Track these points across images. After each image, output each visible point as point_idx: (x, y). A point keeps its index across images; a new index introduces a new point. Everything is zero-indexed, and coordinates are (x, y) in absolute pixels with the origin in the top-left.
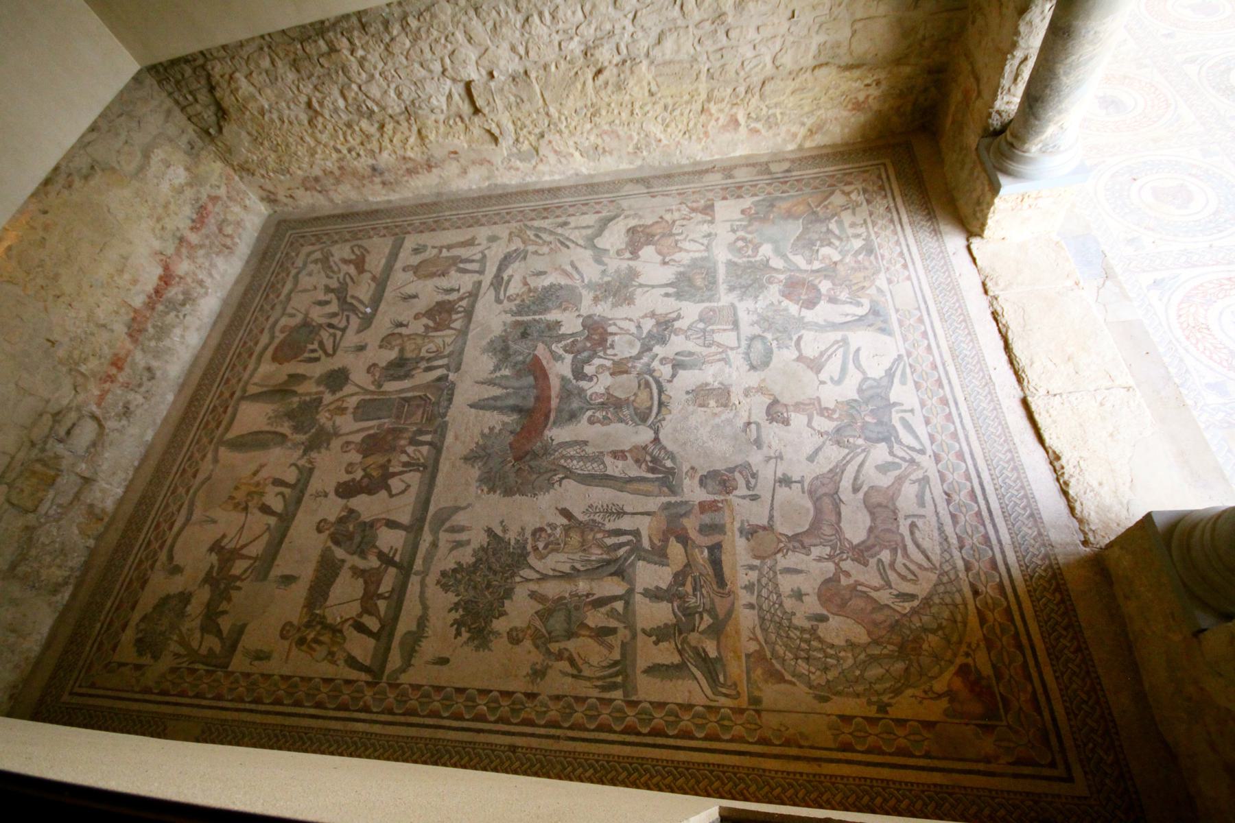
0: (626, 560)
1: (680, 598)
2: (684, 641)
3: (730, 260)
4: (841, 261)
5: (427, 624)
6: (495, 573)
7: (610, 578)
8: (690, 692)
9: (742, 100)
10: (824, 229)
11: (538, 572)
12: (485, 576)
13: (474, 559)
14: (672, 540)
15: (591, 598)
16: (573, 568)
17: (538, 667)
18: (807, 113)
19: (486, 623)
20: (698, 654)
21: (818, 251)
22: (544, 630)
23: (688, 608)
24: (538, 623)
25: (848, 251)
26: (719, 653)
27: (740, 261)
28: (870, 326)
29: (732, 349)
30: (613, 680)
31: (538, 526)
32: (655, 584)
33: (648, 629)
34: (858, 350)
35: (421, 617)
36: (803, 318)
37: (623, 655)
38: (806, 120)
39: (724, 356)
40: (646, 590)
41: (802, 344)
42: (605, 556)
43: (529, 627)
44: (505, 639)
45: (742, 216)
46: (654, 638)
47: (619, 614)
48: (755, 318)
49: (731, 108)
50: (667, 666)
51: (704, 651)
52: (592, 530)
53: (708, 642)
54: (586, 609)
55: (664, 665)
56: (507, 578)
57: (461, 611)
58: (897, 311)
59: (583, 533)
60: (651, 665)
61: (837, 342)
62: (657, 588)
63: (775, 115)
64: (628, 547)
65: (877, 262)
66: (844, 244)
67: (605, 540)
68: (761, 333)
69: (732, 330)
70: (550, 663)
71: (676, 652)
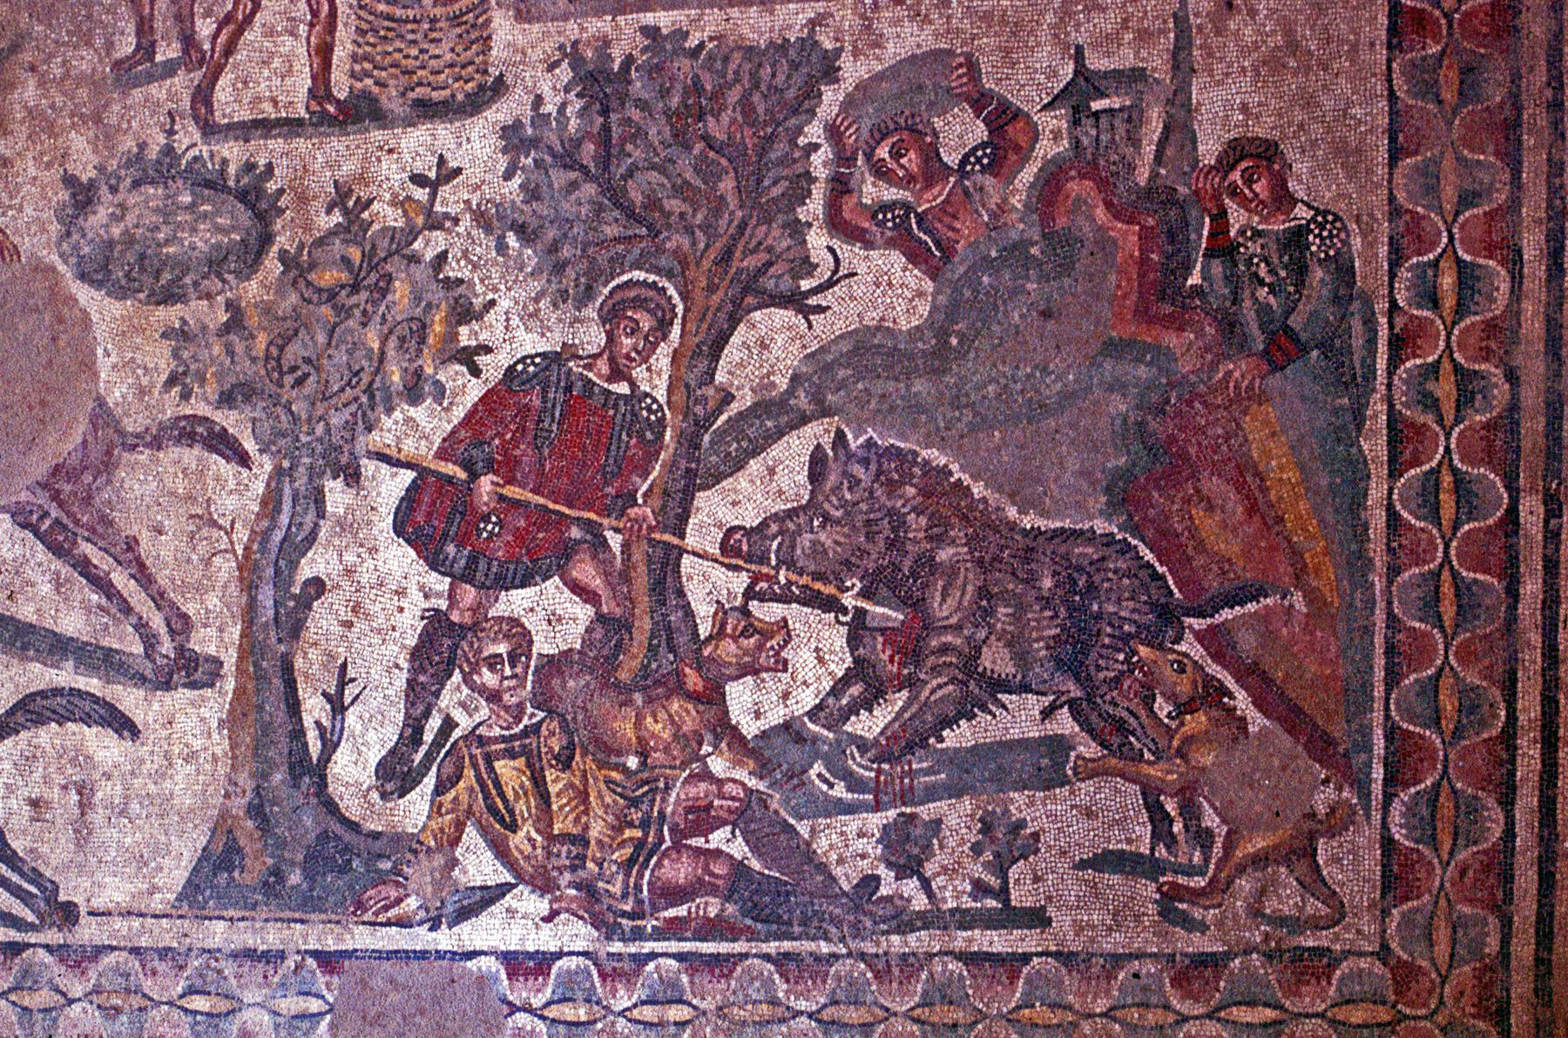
4: (725, 730)
10: (996, 660)
21: (830, 605)
25: (796, 776)
27: (814, 132)
28: (256, 810)
29: (203, 96)
34: (124, 726)
39: (167, 51)
41: (191, 455)
45: (1209, 149)
48: (387, 215)
58: (329, 961)
61: (181, 625)
65: (673, 929)
66: (859, 765)
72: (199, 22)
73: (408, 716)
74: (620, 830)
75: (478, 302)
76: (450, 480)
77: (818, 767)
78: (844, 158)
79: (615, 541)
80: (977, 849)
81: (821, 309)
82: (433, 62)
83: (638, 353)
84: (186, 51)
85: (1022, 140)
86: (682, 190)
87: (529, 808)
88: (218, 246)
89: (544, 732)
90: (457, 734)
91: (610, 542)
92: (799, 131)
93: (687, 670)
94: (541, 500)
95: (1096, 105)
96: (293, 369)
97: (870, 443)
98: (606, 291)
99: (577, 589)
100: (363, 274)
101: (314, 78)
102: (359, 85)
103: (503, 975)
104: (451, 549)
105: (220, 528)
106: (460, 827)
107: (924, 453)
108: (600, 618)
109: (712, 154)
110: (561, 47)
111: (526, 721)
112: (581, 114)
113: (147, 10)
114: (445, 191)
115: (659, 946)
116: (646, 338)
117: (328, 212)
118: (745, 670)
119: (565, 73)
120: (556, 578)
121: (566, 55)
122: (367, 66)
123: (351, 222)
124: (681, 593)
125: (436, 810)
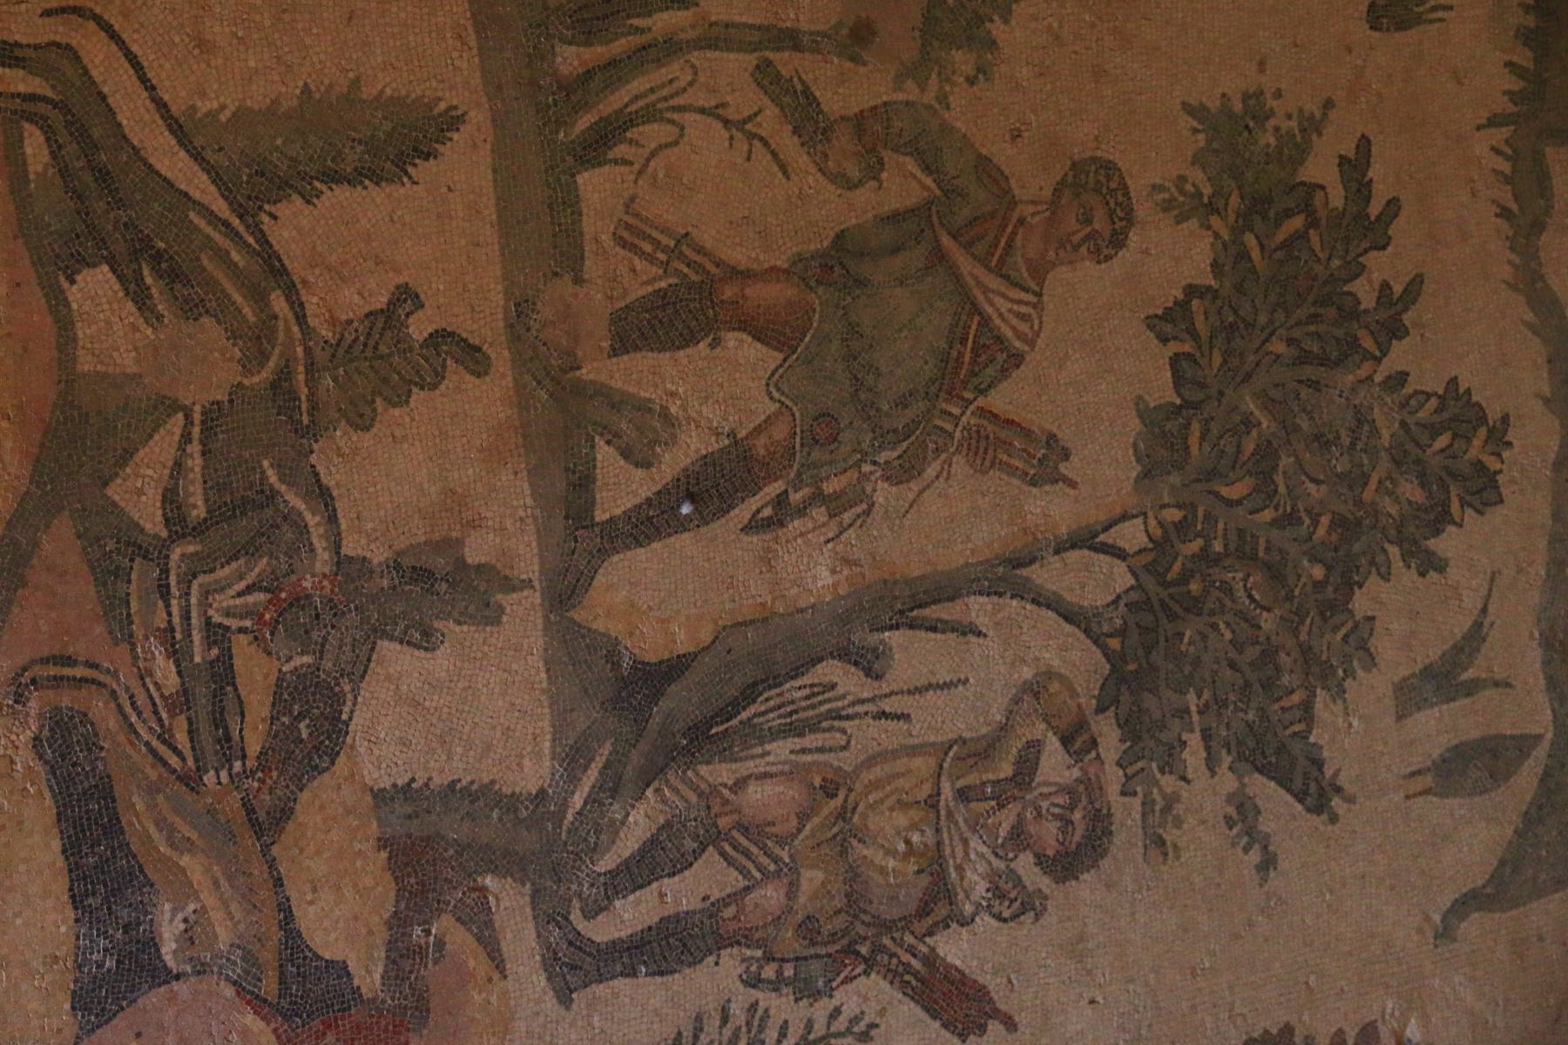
0: (611, 786)
1: (300, 600)
2: (258, 340)
5: (1506, 196)
6: (1244, 551)
7: (683, 645)
8: (204, 45)
11: (1044, 601)
12: (1291, 519)
13: (1361, 604)
14: (369, 978)
15: (758, 502)
16: (870, 663)
17: (963, 61)
19: (1244, 255)
20: (173, 275)
22: (966, 265)
23: (248, 550)
24: (1001, 305)
26: (57, 302)
30: (598, 53)
31: (1087, 886)
32: (441, 661)
33: (456, 376)
35: (1538, 226)
37: (566, 202)
40: (491, 616)
42: (719, 773)
43: (1039, 272)
44: (1137, 187)
46: (419, 328)
47: (613, 438)
50: (334, 178)
51: (142, 299)
52: (808, 928)
53: (127, 361)
54: (780, 432)
55: (355, 178)
56: (1183, 527)
57: (1364, 291)
59: (854, 902)
60: (422, 170)
62: (427, 640)
64: (606, 863)
67: (735, 880)
70: (911, 92)
71: (296, 267)
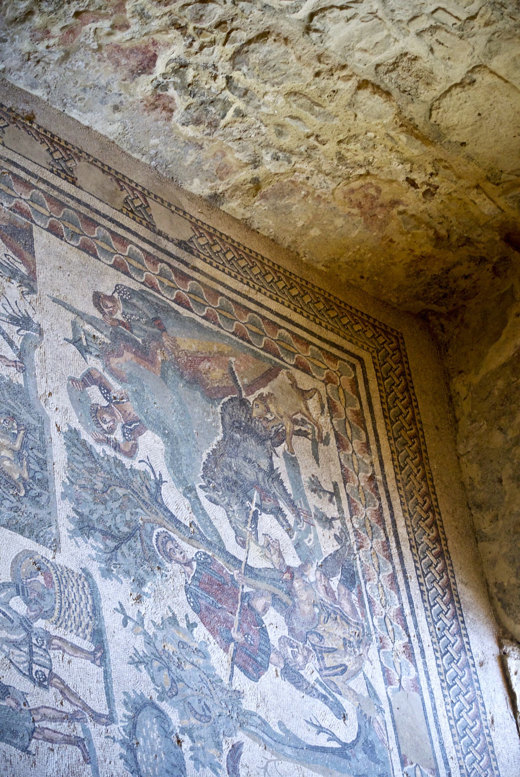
3: (76, 432)
9: (200, 32)
18: (281, 149)
25: (311, 551)
27: (98, 449)
29: (97, 717)
36: (239, 694)
38: (268, 158)
49: (165, 30)
63: (227, 104)
65: (364, 615)
68: (155, 696)
69: (92, 656)
72: (64, 709)
73: (318, 697)
74: (338, 623)
75: (170, 614)
76: (235, 651)
77: (306, 541)
78: (108, 441)
79: (247, 589)
80: (320, 497)
81: (160, 475)
82: (77, 599)
83: (181, 553)
84: (78, 720)
85: (99, 375)
86: (122, 508)
87: (338, 658)
88: (159, 730)
89: (313, 642)
90: (320, 678)
91: (247, 591)
92: (98, 455)
93: (284, 577)
94: (237, 614)
95: (85, 343)
96: (204, 710)
97: (203, 477)
98: (161, 557)
99: (265, 610)
100: (164, 663)
101: (87, 658)
102: (89, 637)
103: (392, 687)
104: (259, 659)
105: (267, 765)
106: (350, 689)
107: (204, 460)
108: (273, 605)
109: (109, 492)
110: (70, 538)
111: (311, 648)
112: (96, 541)
113: (60, 736)
114: (129, 613)
115: (371, 624)
116: (176, 547)
117: (141, 671)
118: (280, 555)
119: (80, 539)
120: (263, 618)
121: (73, 537)
122: (80, 630)
123: (144, 662)
124: (260, 570)
125: (346, 697)
